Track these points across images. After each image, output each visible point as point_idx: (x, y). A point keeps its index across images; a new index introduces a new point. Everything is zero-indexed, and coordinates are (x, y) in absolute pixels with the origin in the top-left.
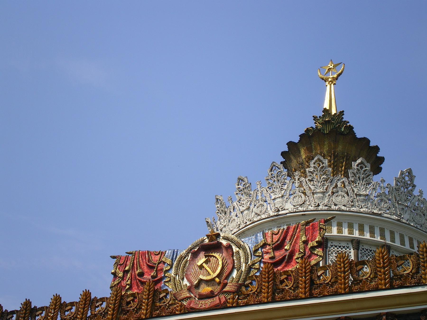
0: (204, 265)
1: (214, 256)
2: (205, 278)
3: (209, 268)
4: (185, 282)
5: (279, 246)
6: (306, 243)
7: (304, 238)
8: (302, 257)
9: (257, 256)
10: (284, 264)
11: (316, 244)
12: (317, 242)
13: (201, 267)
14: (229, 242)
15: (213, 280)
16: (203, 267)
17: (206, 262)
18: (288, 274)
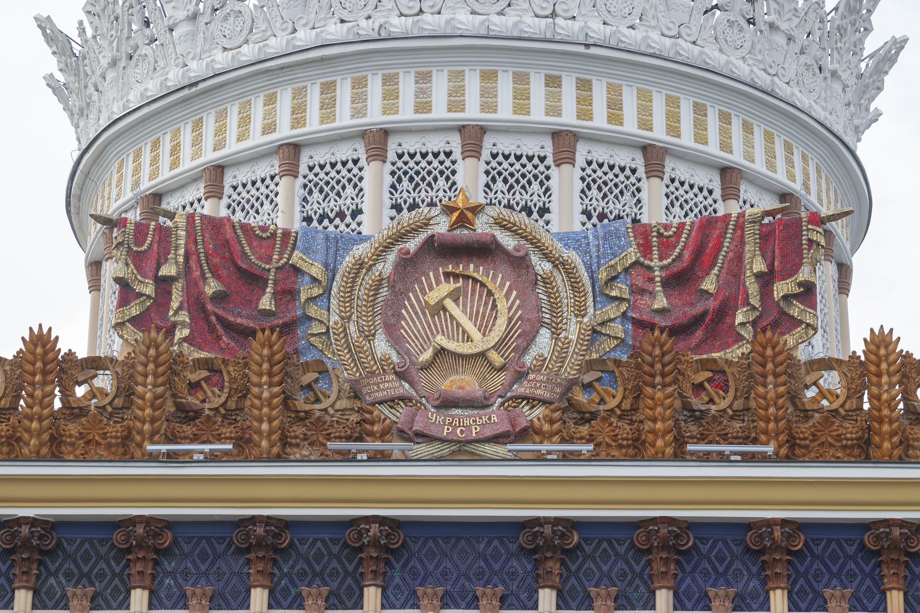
0: (449, 303)
1: (475, 280)
2: (451, 346)
3: (466, 321)
4: (382, 346)
5: (680, 280)
6: (766, 280)
7: (759, 266)
8: (754, 323)
9: (615, 298)
10: (699, 333)
11: (797, 290)
12: (800, 284)
13: (440, 307)
14: (523, 242)
15: (483, 354)
16: (445, 309)
17: (454, 296)
18: (714, 368)
